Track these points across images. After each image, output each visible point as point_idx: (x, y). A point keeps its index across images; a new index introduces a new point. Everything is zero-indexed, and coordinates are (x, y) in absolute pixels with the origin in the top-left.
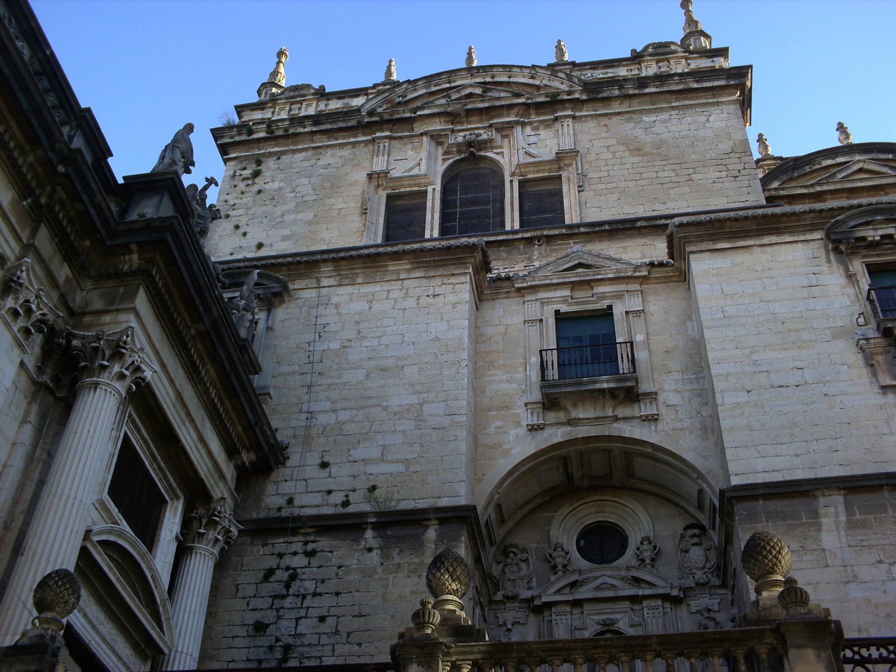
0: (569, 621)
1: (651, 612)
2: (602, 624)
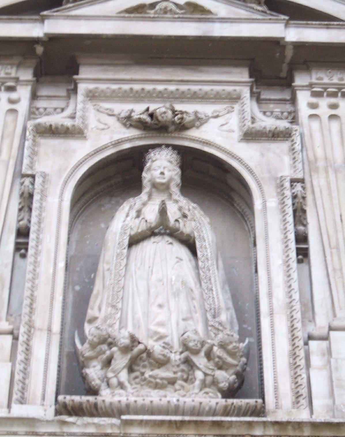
0: (23, 107)
1: (324, 103)
2: (141, 125)
